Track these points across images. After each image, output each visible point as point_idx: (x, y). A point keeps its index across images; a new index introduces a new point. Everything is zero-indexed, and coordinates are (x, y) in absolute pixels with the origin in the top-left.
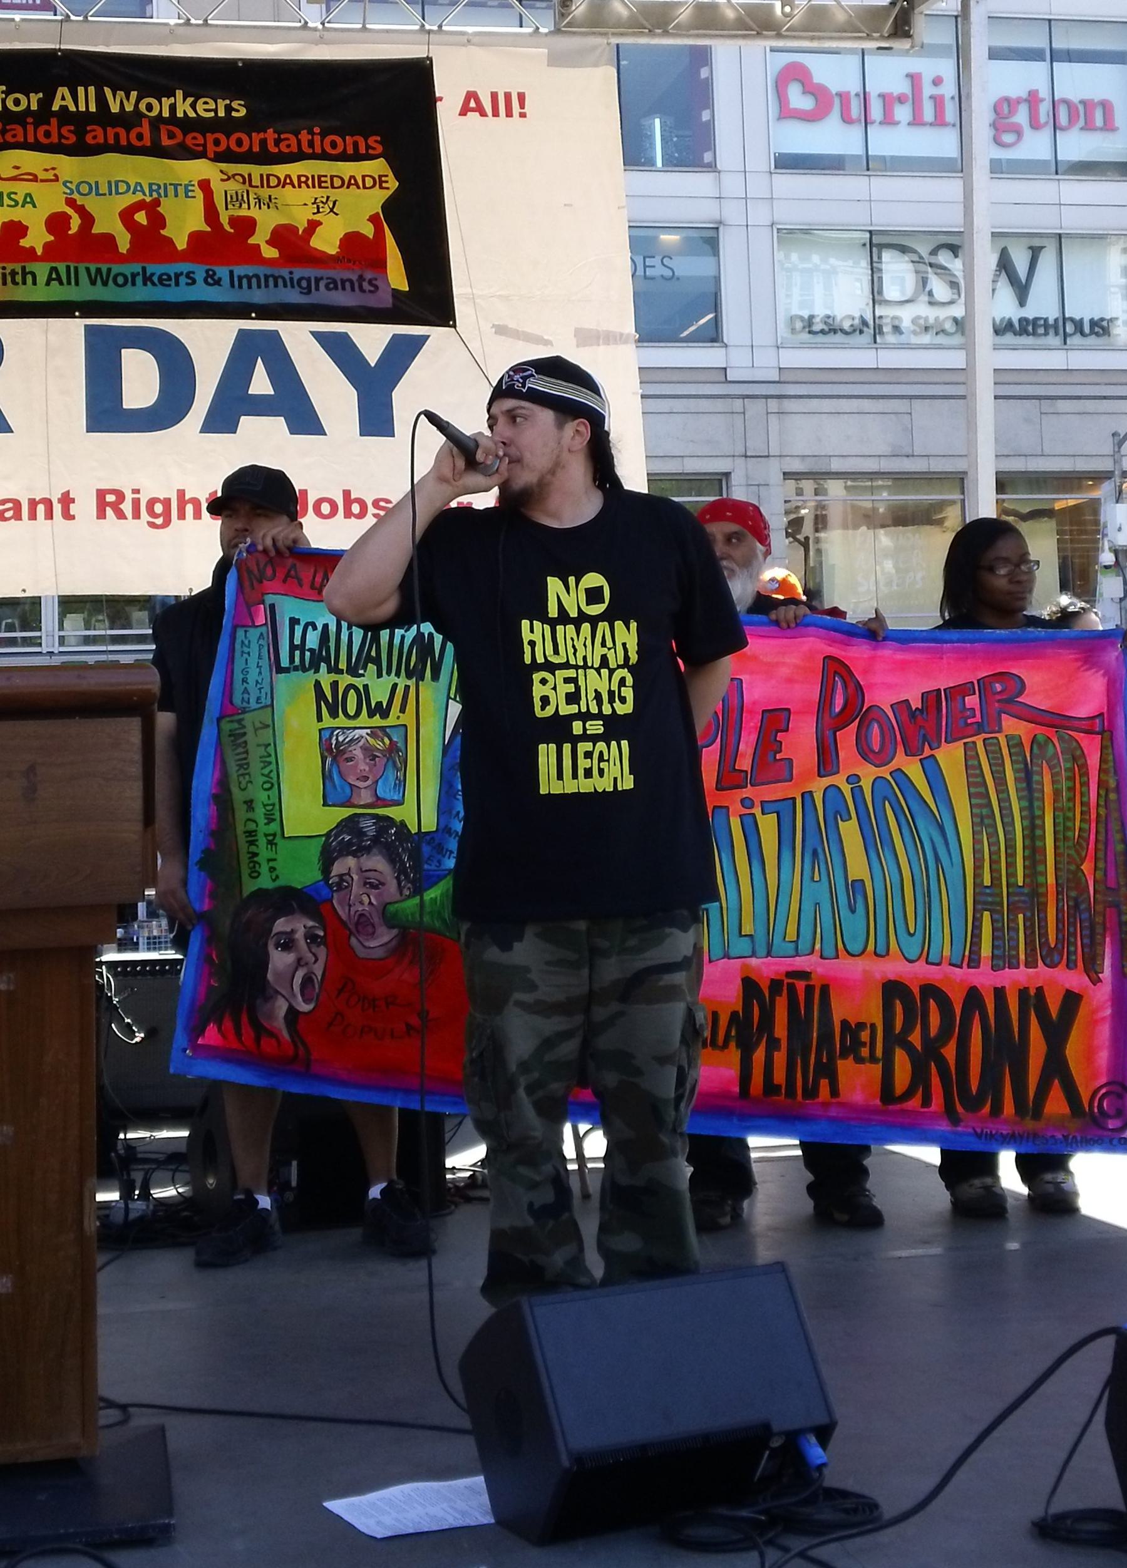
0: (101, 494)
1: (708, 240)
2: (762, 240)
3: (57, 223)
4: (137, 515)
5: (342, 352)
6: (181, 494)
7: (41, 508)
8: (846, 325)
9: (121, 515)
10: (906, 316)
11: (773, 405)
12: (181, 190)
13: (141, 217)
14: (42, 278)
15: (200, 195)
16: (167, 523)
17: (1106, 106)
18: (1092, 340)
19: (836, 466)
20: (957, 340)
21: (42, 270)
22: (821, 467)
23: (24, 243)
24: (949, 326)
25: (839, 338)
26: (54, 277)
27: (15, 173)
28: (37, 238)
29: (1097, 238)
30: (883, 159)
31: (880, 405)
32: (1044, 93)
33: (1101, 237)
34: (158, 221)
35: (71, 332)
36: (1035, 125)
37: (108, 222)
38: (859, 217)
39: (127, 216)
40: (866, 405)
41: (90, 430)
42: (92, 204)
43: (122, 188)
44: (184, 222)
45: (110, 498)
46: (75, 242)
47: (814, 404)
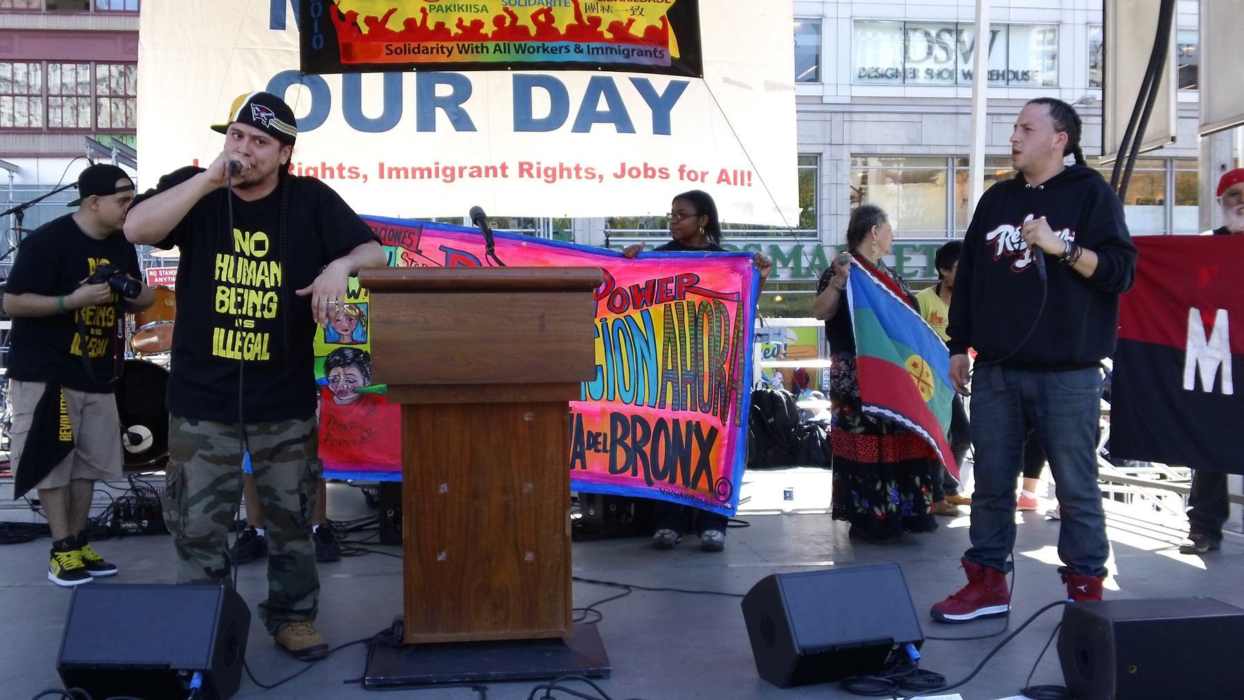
0: (521, 164)
1: (815, 26)
2: (846, 25)
3: (499, 21)
4: (539, 176)
6: (561, 165)
7: (491, 172)
9: (531, 176)
10: (921, 69)
11: (847, 117)
13: (542, 18)
14: (491, 49)
16: (554, 181)
18: (1022, 83)
19: (879, 150)
20: (949, 82)
21: (491, 45)
22: (872, 150)
23: (482, 31)
25: (884, 80)
28: (489, 29)
29: (1026, 27)
33: (1028, 26)
34: (550, 19)
35: (506, 78)
37: (525, 20)
39: (534, 17)
41: (516, 130)
42: (516, 10)
45: (526, 167)
47: (870, 117)
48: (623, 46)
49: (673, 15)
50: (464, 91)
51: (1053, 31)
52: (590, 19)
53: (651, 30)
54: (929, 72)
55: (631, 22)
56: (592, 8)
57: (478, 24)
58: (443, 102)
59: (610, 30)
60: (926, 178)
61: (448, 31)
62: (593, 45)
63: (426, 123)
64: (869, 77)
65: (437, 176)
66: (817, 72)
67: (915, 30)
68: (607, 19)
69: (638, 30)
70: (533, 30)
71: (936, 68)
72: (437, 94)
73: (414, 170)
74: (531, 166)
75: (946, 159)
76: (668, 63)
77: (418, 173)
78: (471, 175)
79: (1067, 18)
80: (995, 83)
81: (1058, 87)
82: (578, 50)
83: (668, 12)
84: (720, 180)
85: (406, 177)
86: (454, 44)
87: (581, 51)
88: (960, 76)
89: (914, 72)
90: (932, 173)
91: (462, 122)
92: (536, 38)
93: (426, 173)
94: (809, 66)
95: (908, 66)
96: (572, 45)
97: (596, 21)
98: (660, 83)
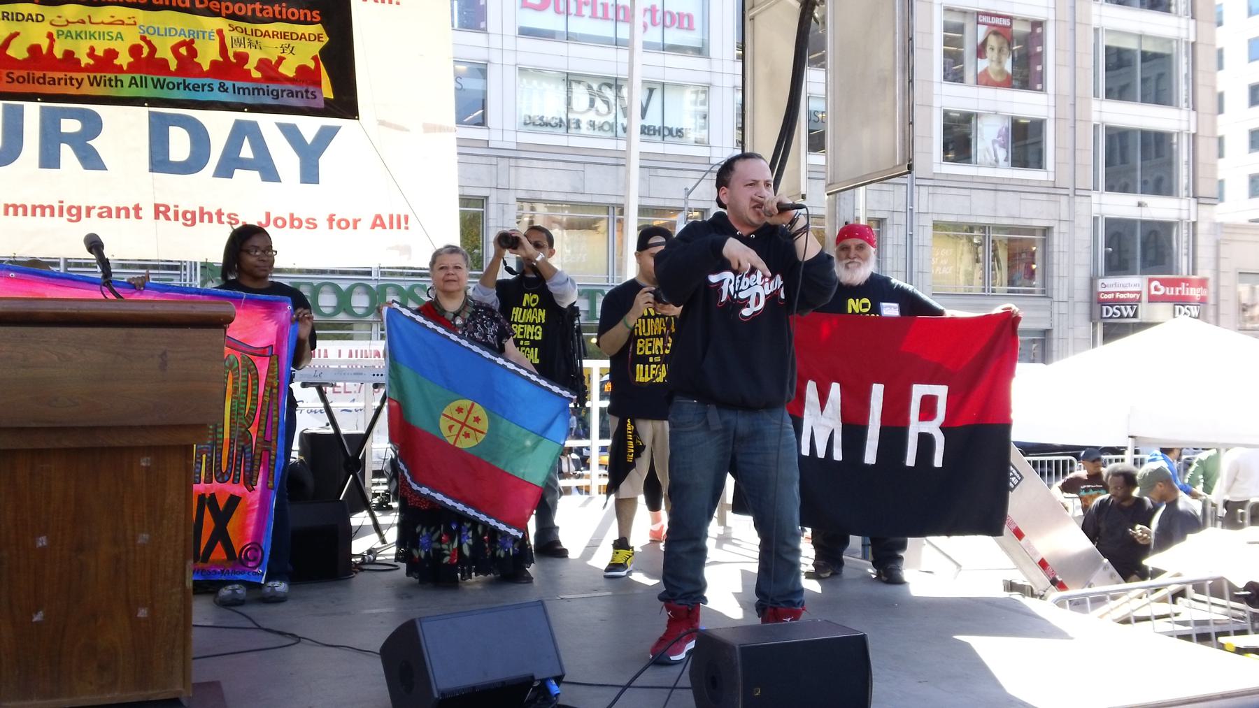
1: (481, 71)
2: (511, 73)
3: (135, 50)
5: (292, 134)
7: (123, 213)
8: (553, 123)
10: (584, 120)
11: (513, 162)
12: (207, 35)
13: (183, 51)
14: (126, 83)
15: (217, 38)
17: (690, 17)
18: (677, 139)
19: (544, 196)
21: (126, 78)
22: (537, 196)
23: (117, 62)
24: (606, 127)
25: (549, 129)
26: (133, 82)
27: (112, 20)
28: (124, 59)
29: (680, 86)
30: (575, 34)
31: (570, 166)
32: (659, 7)
34: (193, 53)
36: (654, 24)
38: (563, 66)
39: (175, 50)
40: (561, 165)
42: (155, 40)
43: (173, 32)
44: (208, 54)
46: (145, 62)
47: (535, 163)
48: (272, 86)
49: (325, 54)
50: (93, 126)
51: (704, 92)
52: (236, 55)
53: (302, 69)
54: (592, 125)
55: (281, 60)
56: (239, 42)
57: (112, 54)
58: (70, 139)
59: (257, 68)
60: (589, 225)
61: (78, 61)
62: (239, 84)
63: (49, 159)
64: (534, 124)
65: (61, 214)
66: (484, 116)
67: (579, 82)
68: (254, 57)
69: (288, 70)
70: (173, 65)
71: (599, 120)
72: (63, 130)
73: (34, 208)
74: (168, 209)
75: (607, 208)
76: (322, 105)
77: (38, 210)
78: (100, 215)
79: (717, 80)
80: (653, 138)
81: (708, 145)
82: (223, 89)
83: (322, 52)
84: (374, 226)
85: (25, 214)
86: (84, 75)
87: (226, 90)
88: (620, 129)
89: (578, 123)
90: (596, 221)
91: (91, 160)
92: (177, 73)
93: (48, 211)
94: (473, 109)
95: (571, 116)
96: (216, 83)
97: (243, 58)
98: (309, 126)
